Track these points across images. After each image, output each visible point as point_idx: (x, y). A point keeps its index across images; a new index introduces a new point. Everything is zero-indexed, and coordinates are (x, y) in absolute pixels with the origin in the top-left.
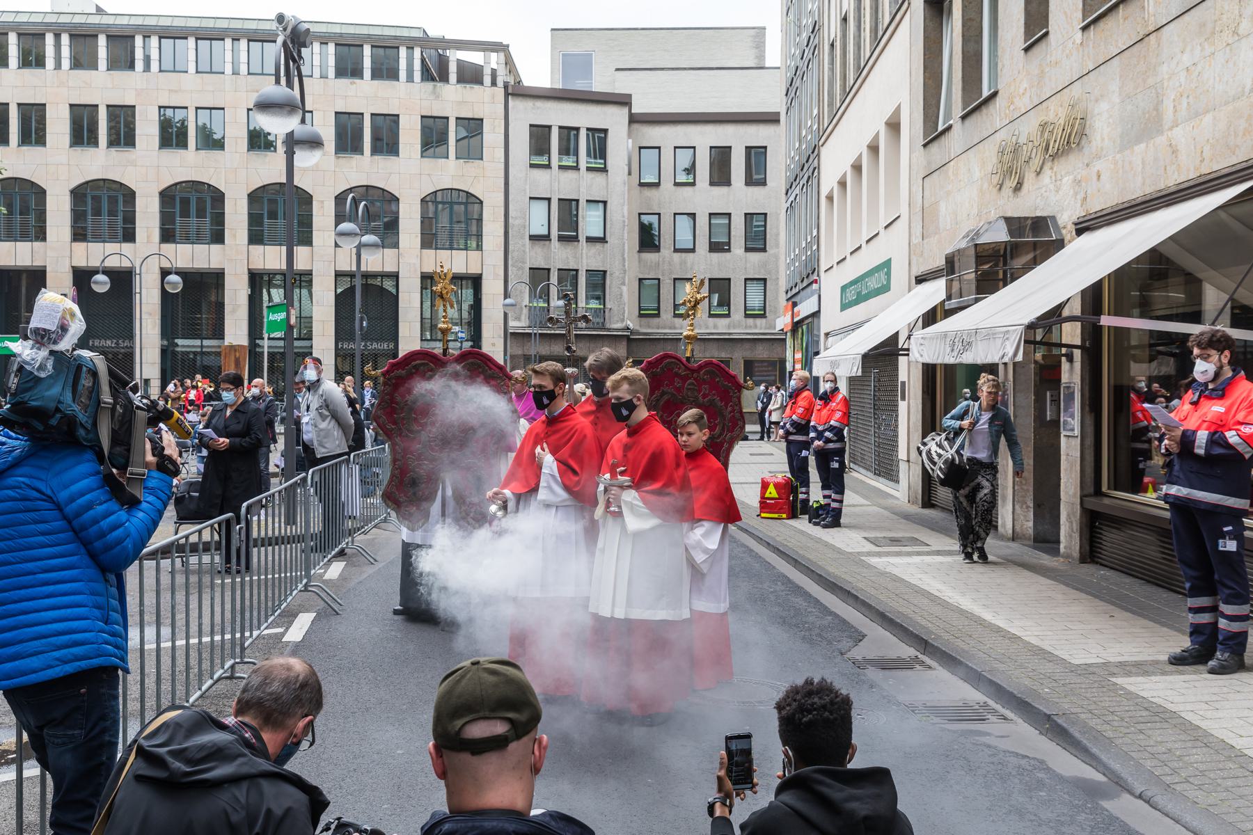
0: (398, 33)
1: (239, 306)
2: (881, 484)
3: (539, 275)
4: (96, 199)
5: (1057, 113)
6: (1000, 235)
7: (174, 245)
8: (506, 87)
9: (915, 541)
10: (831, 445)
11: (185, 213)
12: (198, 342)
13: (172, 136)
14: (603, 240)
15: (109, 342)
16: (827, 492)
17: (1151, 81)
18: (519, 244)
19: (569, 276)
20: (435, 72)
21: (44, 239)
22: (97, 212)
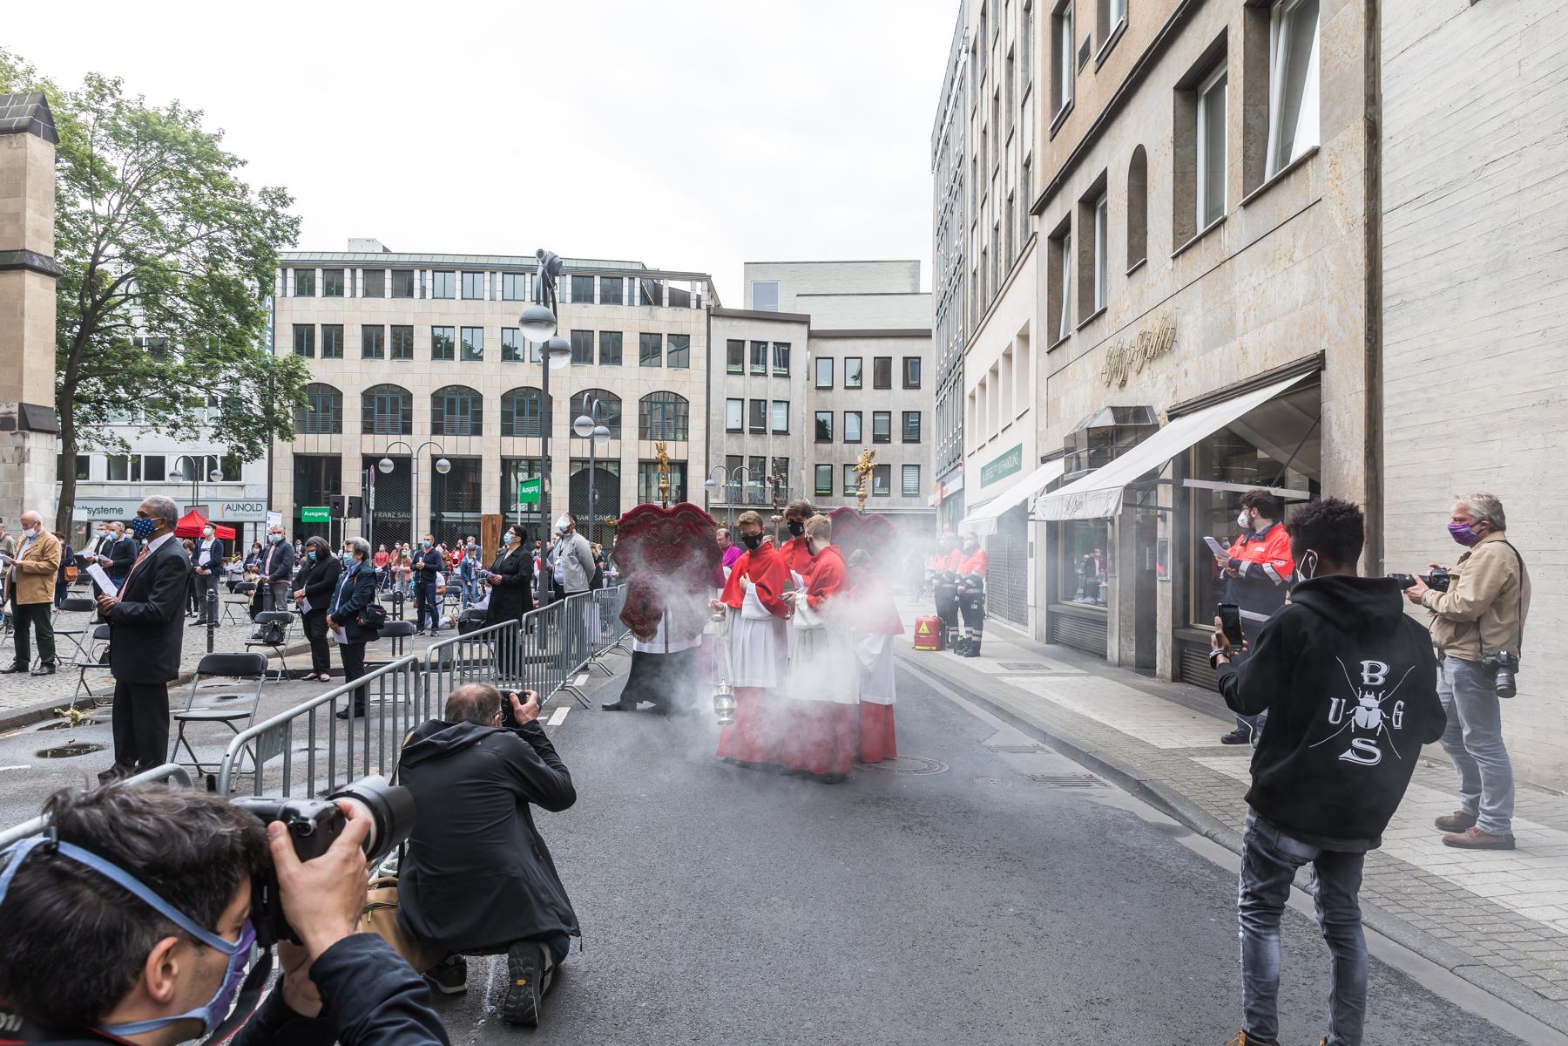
0: (623, 266)
1: (493, 485)
2: (1014, 627)
3: (734, 461)
5: (1153, 324)
6: (1108, 420)
8: (708, 309)
9: (1040, 667)
10: (971, 591)
11: (451, 411)
12: (459, 515)
13: (442, 350)
14: (786, 433)
15: (389, 514)
16: (969, 629)
17: (1226, 298)
18: (719, 436)
19: (758, 462)
20: (652, 297)
21: (340, 432)
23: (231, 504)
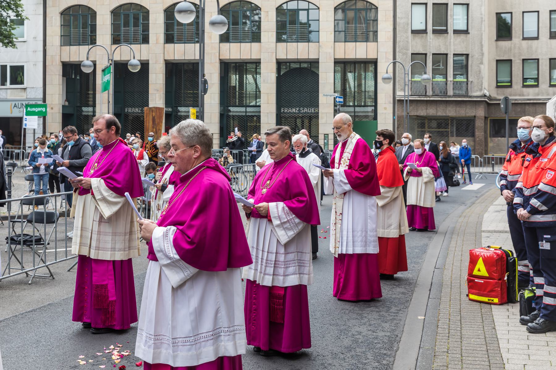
4: (127, 16)
7: (173, 45)
14: (466, 32)
18: (404, 36)
22: (126, 24)
23: (17, 103)
